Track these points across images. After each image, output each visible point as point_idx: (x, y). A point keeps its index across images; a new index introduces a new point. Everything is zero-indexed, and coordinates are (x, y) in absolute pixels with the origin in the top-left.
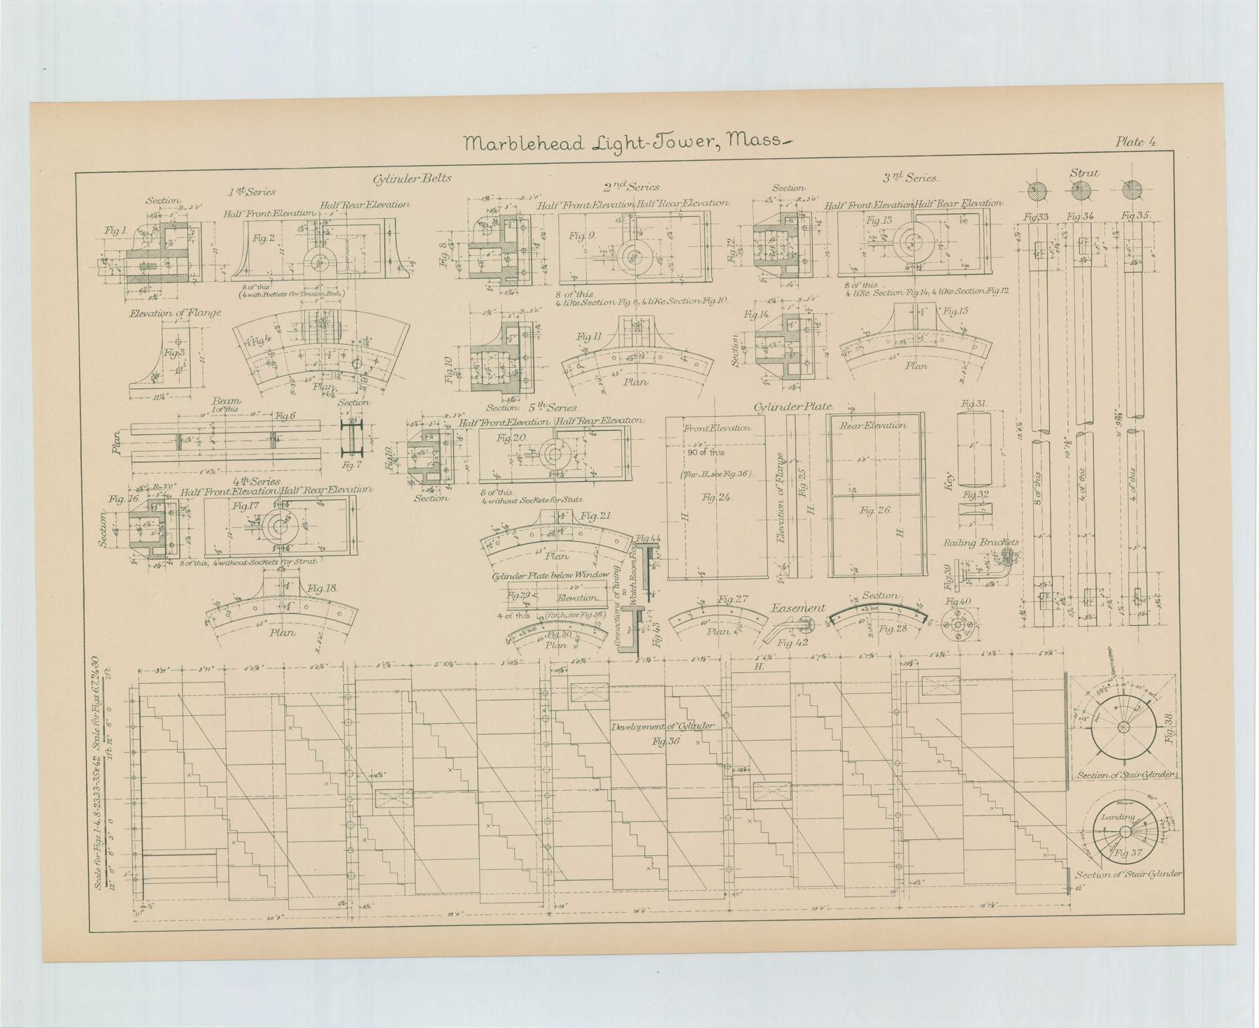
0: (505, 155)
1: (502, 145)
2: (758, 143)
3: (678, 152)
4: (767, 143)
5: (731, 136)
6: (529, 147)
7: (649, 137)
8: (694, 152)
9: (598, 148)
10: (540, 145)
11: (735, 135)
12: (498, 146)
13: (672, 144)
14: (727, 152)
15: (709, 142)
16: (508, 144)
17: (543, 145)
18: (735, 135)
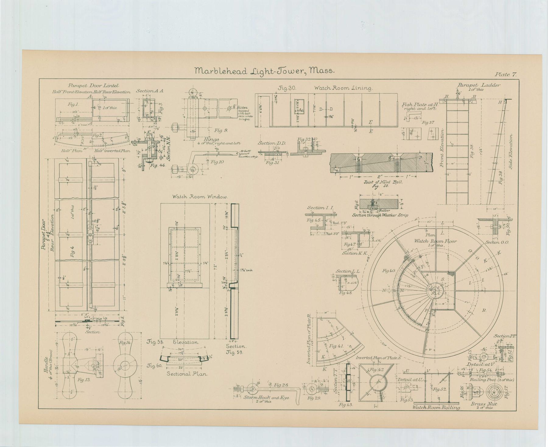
0: (213, 75)
1: (211, 72)
2: (323, 72)
3: (288, 76)
4: (327, 72)
5: (311, 69)
6: (223, 73)
7: (275, 69)
9: (253, 73)
10: (228, 72)
12: (209, 72)
14: (309, 76)
15: (301, 71)
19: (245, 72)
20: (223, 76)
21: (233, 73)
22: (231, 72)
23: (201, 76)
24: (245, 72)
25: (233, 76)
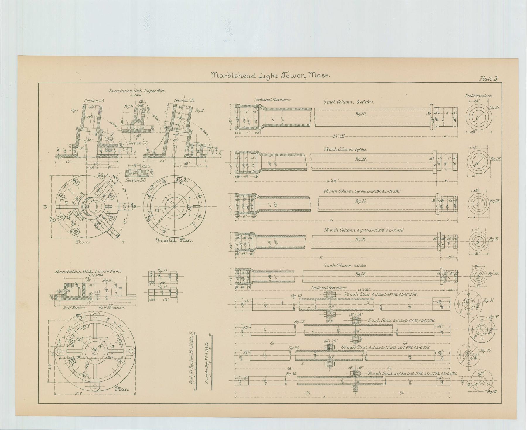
0: (226, 79)
4: (323, 76)
5: (310, 74)
8: (296, 79)
9: (261, 77)
10: (239, 76)
11: (311, 73)
12: (224, 76)
13: (288, 76)
16: (227, 75)
18: (311, 73)
19: (254, 76)
20: (235, 80)
21: (244, 77)
22: (242, 76)
24: (254, 76)
25: (243, 80)
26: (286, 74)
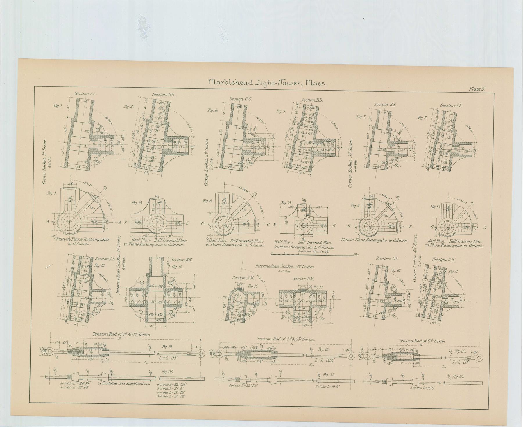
0: (223, 86)
2: (316, 85)
3: (287, 87)
4: (320, 85)
6: (232, 83)
8: (293, 87)
9: (258, 84)
10: (236, 83)
11: (308, 81)
12: (221, 83)
13: (285, 84)
14: (305, 87)
15: (298, 84)
16: (225, 82)
17: (237, 83)
18: (308, 81)
19: (251, 83)
20: (232, 86)
21: (241, 83)
23: (213, 86)
24: (251, 83)
26: (283, 81)
